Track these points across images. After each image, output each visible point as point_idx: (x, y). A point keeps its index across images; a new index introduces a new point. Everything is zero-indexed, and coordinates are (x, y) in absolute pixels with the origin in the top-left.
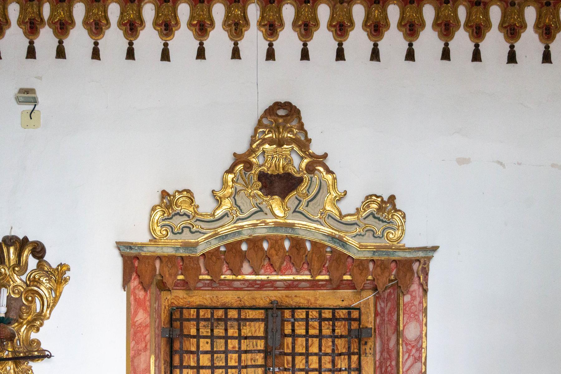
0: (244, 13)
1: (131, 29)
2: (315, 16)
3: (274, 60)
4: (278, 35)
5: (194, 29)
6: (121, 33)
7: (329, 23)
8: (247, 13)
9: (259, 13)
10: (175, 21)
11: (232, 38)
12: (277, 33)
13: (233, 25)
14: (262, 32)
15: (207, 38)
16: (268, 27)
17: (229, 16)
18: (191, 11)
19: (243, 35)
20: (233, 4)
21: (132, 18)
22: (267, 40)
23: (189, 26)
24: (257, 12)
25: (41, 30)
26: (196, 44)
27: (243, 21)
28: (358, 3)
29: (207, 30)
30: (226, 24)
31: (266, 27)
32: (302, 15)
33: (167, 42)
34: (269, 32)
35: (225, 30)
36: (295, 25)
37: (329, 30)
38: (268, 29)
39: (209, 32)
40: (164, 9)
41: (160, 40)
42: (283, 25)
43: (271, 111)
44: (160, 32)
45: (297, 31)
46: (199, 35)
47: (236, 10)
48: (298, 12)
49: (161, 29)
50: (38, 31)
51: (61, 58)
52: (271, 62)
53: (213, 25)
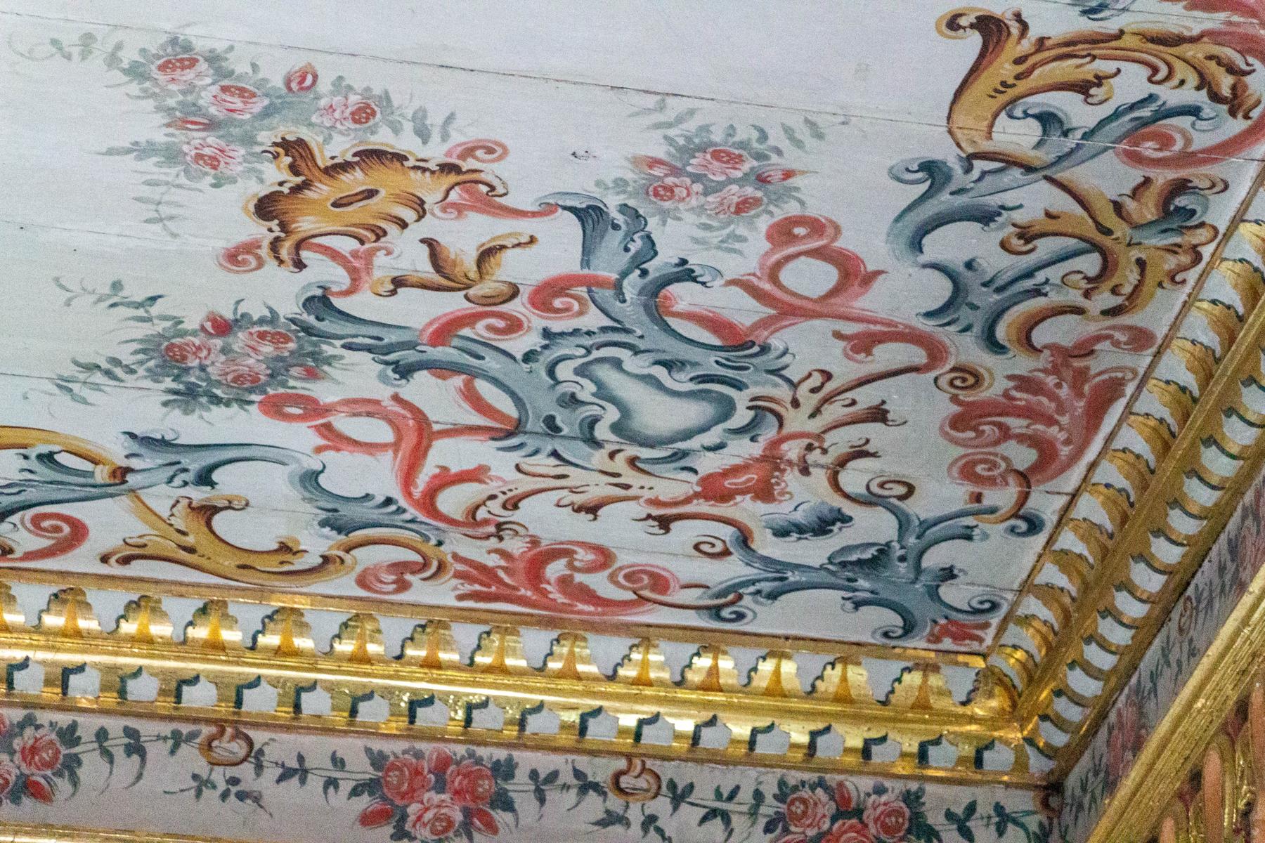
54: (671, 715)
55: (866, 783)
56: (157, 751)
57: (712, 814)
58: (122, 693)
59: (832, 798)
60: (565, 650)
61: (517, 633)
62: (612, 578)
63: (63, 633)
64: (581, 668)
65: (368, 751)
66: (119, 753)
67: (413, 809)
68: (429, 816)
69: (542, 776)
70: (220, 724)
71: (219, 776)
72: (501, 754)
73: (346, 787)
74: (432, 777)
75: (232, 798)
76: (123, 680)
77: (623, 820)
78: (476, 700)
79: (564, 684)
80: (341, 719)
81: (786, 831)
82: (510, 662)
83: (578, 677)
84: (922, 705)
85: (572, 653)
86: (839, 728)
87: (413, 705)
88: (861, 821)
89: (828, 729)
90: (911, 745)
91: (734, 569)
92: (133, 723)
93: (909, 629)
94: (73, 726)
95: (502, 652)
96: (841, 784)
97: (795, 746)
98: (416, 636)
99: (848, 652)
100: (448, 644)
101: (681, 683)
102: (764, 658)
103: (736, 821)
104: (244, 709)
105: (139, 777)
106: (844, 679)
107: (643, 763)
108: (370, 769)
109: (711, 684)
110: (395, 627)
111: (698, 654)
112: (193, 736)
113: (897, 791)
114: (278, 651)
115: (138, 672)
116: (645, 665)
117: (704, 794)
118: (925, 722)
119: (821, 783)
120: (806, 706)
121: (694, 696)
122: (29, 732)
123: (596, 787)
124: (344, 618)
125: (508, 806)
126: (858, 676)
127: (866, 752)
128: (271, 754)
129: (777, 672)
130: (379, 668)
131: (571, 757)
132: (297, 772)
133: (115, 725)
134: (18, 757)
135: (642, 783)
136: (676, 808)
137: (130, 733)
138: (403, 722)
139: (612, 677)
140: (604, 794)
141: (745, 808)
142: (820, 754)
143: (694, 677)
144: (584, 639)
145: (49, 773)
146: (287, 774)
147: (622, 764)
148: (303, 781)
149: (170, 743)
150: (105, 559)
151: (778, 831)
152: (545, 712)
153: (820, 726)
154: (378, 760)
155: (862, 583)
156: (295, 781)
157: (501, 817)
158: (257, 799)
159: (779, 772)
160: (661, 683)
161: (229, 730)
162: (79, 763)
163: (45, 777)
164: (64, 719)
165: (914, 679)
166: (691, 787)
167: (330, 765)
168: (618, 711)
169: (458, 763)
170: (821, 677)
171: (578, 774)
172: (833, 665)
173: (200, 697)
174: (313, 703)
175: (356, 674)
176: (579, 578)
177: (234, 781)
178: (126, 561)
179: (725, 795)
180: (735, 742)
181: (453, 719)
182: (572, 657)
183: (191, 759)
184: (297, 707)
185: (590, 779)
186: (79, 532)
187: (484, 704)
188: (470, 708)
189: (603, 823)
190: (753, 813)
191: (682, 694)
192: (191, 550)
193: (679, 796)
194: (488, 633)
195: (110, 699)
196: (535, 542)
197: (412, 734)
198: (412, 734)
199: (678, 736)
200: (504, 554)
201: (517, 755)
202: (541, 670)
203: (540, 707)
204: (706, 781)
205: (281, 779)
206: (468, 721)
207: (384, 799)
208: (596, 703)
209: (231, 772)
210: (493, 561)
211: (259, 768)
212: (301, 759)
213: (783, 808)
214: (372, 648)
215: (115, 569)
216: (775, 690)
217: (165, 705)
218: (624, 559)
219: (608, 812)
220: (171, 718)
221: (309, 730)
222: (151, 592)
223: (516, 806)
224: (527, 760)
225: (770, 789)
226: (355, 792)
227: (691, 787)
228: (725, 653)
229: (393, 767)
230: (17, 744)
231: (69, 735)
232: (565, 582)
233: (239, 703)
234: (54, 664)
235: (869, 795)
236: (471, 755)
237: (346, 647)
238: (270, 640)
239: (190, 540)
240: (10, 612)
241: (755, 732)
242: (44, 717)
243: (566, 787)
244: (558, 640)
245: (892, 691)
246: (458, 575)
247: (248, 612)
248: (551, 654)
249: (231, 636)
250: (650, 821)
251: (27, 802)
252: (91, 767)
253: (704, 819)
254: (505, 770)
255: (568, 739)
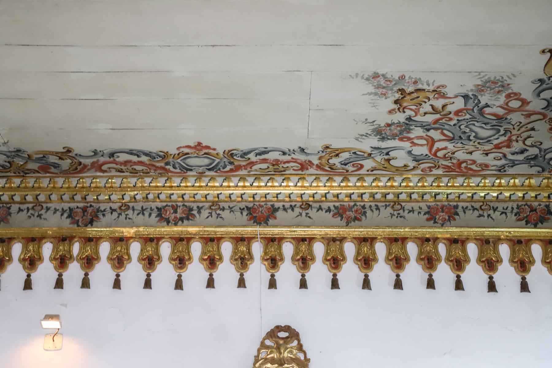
0: (249, 250)
1: (149, 264)
2: (312, 252)
3: (276, 288)
4: (279, 268)
5: (205, 263)
6: (140, 266)
7: (324, 258)
8: (251, 249)
9: (262, 249)
10: (188, 256)
11: (238, 270)
12: (278, 265)
13: (239, 259)
14: (265, 265)
15: (217, 271)
16: (270, 261)
17: (236, 252)
18: (203, 249)
19: (248, 267)
20: (239, 243)
21: (150, 254)
22: (269, 272)
23: (200, 261)
24: (260, 249)
25: (70, 265)
26: (206, 275)
27: (248, 256)
28: (349, 241)
29: (216, 264)
30: (233, 259)
31: (268, 261)
32: (300, 251)
33: (181, 273)
34: (271, 265)
35: (232, 264)
36: (293, 259)
37: (324, 263)
38: (270, 263)
39: (218, 265)
40: (179, 247)
41: (175, 272)
42: (283, 259)
43: (272, 334)
44: (174, 266)
45: (295, 265)
46: (209, 268)
47: (242, 247)
48: (296, 249)
49: (176, 263)
50: (67, 265)
51: (85, 288)
52: (273, 290)
53: (221, 260)
54: (492, 193)
55: (536, 204)
56: (382, 209)
57: (502, 213)
58: (374, 197)
59: (529, 207)
60: (467, 181)
61: (456, 178)
62: (476, 166)
63: (361, 186)
64: (471, 184)
65: (427, 205)
66: (374, 210)
67: (437, 217)
68: (441, 218)
69: (464, 208)
70: (395, 202)
71: (395, 213)
72: (455, 204)
73: (423, 213)
74: (441, 210)
75: (399, 217)
76: (374, 195)
77: (483, 216)
78: (449, 193)
79: (468, 188)
80: (420, 199)
81: (519, 215)
82: (455, 185)
83: (471, 186)
84: (548, 186)
85: (469, 181)
86: (529, 192)
87: (435, 195)
88: (536, 212)
89: (527, 193)
90: (546, 195)
91: (503, 162)
92: (376, 203)
93: (543, 170)
94: (364, 205)
95: (453, 183)
96: (531, 204)
97: (520, 197)
98: (435, 181)
99: (530, 177)
100: (442, 182)
101: (493, 186)
102: (511, 179)
103: (508, 214)
104: (400, 199)
105: (379, 215)
106: (530, 182)
107: (486, 203)
108: (427, 209)
109: (500, 185)
110: (430, 179)
111: (496, 179)
112: (389, 205)
113: (544, 205)
114: (406, 186)
115: (377, 193)
116: (485, 183)
117: (500, 209)
118: (549, 190)
119: (526, 204)
120: (522, 188)
121: (496, 188)
122: (355, 207)
123: (476, 209)
124: (419, 178)
125: (458, 214)
126: (533, 181)
127: (536, 197)
128: (406, 208)
129: (514, 182)
130: (427, 188)
131: (470, 203)
132: (412, 211)
133: (373, 204)
134: (354, 213)
135: (486, 207)
136: (494, 212)
137: (376, 206)
138: (434, 199)
139: (478, 186)
140: (478, 211)
141: (510, 211)
142: (525, 198)
143: (496, 184)
144: (471, 178)
145: (360, 215)
146: (410, 212)
147: (482, 204)
148: (413, 213)
149: (385, 207)
150: (368, 171)
151: (518, 215)
152: (464, 194)
153: (525, 192)
154: (429, 207)
155: (532, 162)
156: (412, 212)
157: (456, 217)
158: (404, 217)
159: (517, 203)
160: (489, 186)
161: (397, 203)
162: (366, 213)
163: (360, 216)
164: (362, 204)
165: (545, 181)
166: (497, 208)
167: (418, 209)
168: (480, 193)
169: (446, 206)
170: (524, 182)
171: (472, 207)
172: (527, 179)
173: (390, 197)
174: (414, 196)
175: (423, 190)
176: (469, 166)
177: (399, 214)
178: (372, 171)
179: (505, 209)
180: (506, 197)
181: (444, 197)
182: (469, 183)
183: (389, 210)
184: (411, 197)
185: (475, 207)
186: (362, 166)
187: (451, 194)
188: (447, 195)
189: (479, 217)
190: (512, 212)
191: (493, 188)
192: (386, 168)
193: (495, 210)
194: (450, 179)
195: (371, 199)
196: (459, 160)
197: (435, 201)
198: (435, 201)
199: (493, 197)
200: (452, 163)
201: (459, 203)
202: (462, 186)
203: (463, 193)
204: (501, 206)
205: (409, 213)
206: (447, 197)
207: (431, 215)
208: (475, 191)
209: (398, 212)
210: (450, 165)
211: (404, 211)
212: (412, 208)
213: (518, 210)
214: (425, 184)
215: (370, 173)
216: (514, 185)
217: (383, 199)
218: (479, 162)
219: (479, 214)
220: (384, 202)
221: (413, 202)
222: (378, 176)
223: (460, 214)
224: (461, 204)
225: (515, 207)
226: (425, 214)
227: (497, 208)
228: (502, 179)
229: (432, 208)
230: (353, 210)
231: (364, 207)
232: (466, 168)
233: (398, 197)
234: (359, 193)
235: (537, 206)
236: (449, 204)
237: (420, 184)
238: (404, 184)
239: (385, 166)
240: (349, 183)
241: (510, 195)
242: (358, 204)
243: (470, 210)
244: (465, 179)
245: (541, 184)
246: (442, 168)
247: (399, 179)
248: (464, 182)
249: (395, 184)
250: (489, 216)
251: (356, 221)
252: (369, 213)
253: (501, 214)
254: (456, 207)
255: (470, 199)
